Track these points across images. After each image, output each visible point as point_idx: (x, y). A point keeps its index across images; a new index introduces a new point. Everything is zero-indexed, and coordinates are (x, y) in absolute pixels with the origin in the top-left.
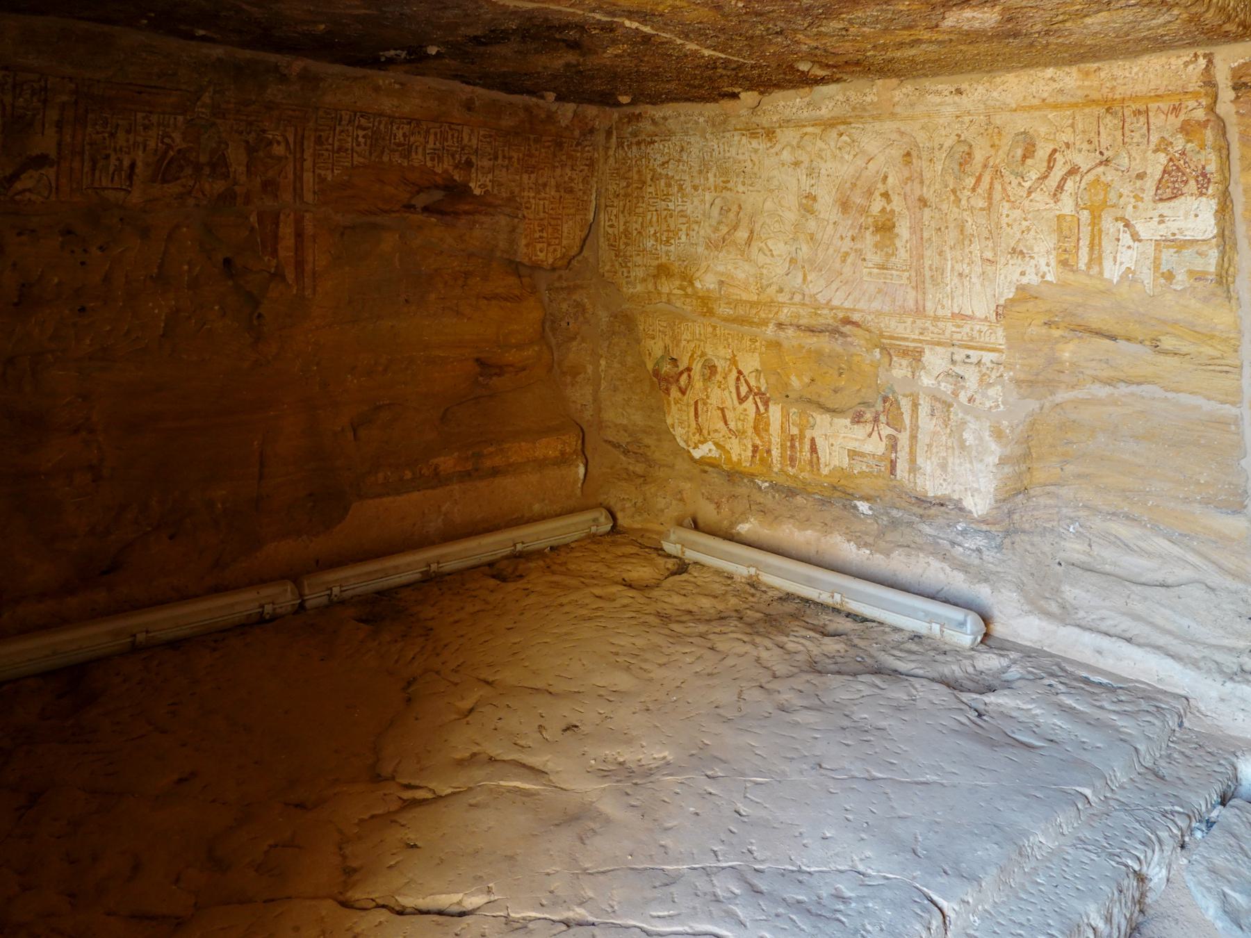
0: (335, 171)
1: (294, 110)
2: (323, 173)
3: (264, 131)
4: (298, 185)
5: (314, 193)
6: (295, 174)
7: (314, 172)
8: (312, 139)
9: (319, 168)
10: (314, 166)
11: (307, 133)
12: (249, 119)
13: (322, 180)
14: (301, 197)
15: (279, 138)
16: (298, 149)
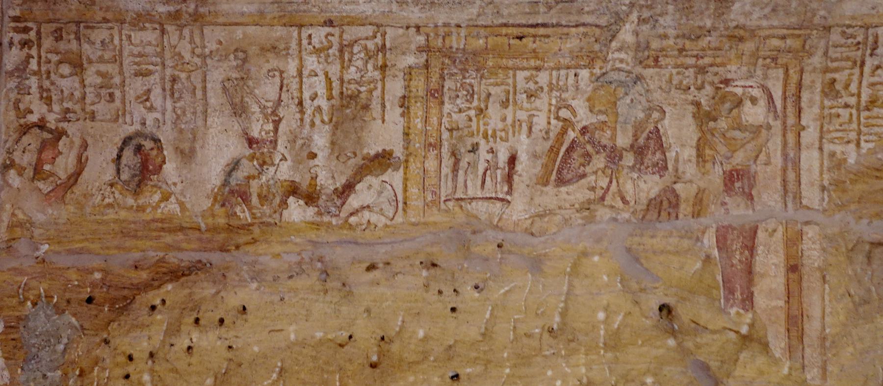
0: (863, 144)
1: (783, 38)
2: (838, 149)
3: (727, 82)
4: (791, 176)
5: (823, 189)
6: (785, 156)
7: (821, 149)
8: (818, 87)
9: (832, 141)
10: (821, 138)
11: (807, 79)
12: (701, 62)
13: (839, 164)
14: (798, 197)
15: (756, 92)
16: (790, 110)
